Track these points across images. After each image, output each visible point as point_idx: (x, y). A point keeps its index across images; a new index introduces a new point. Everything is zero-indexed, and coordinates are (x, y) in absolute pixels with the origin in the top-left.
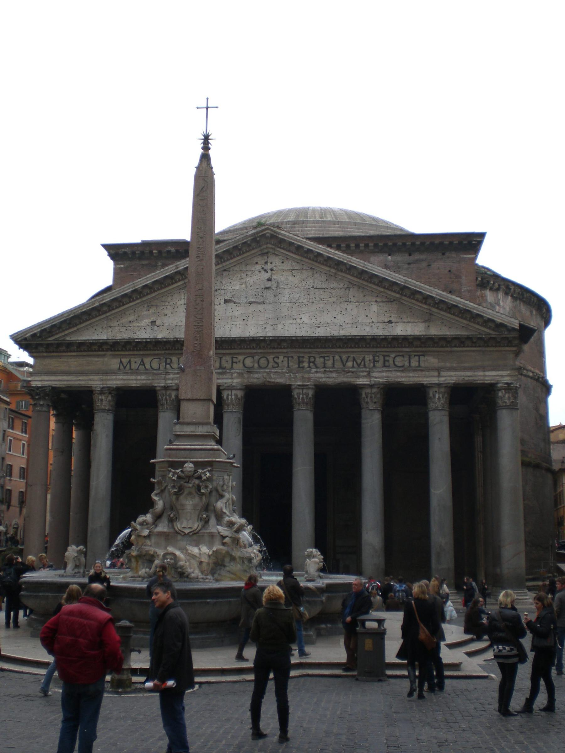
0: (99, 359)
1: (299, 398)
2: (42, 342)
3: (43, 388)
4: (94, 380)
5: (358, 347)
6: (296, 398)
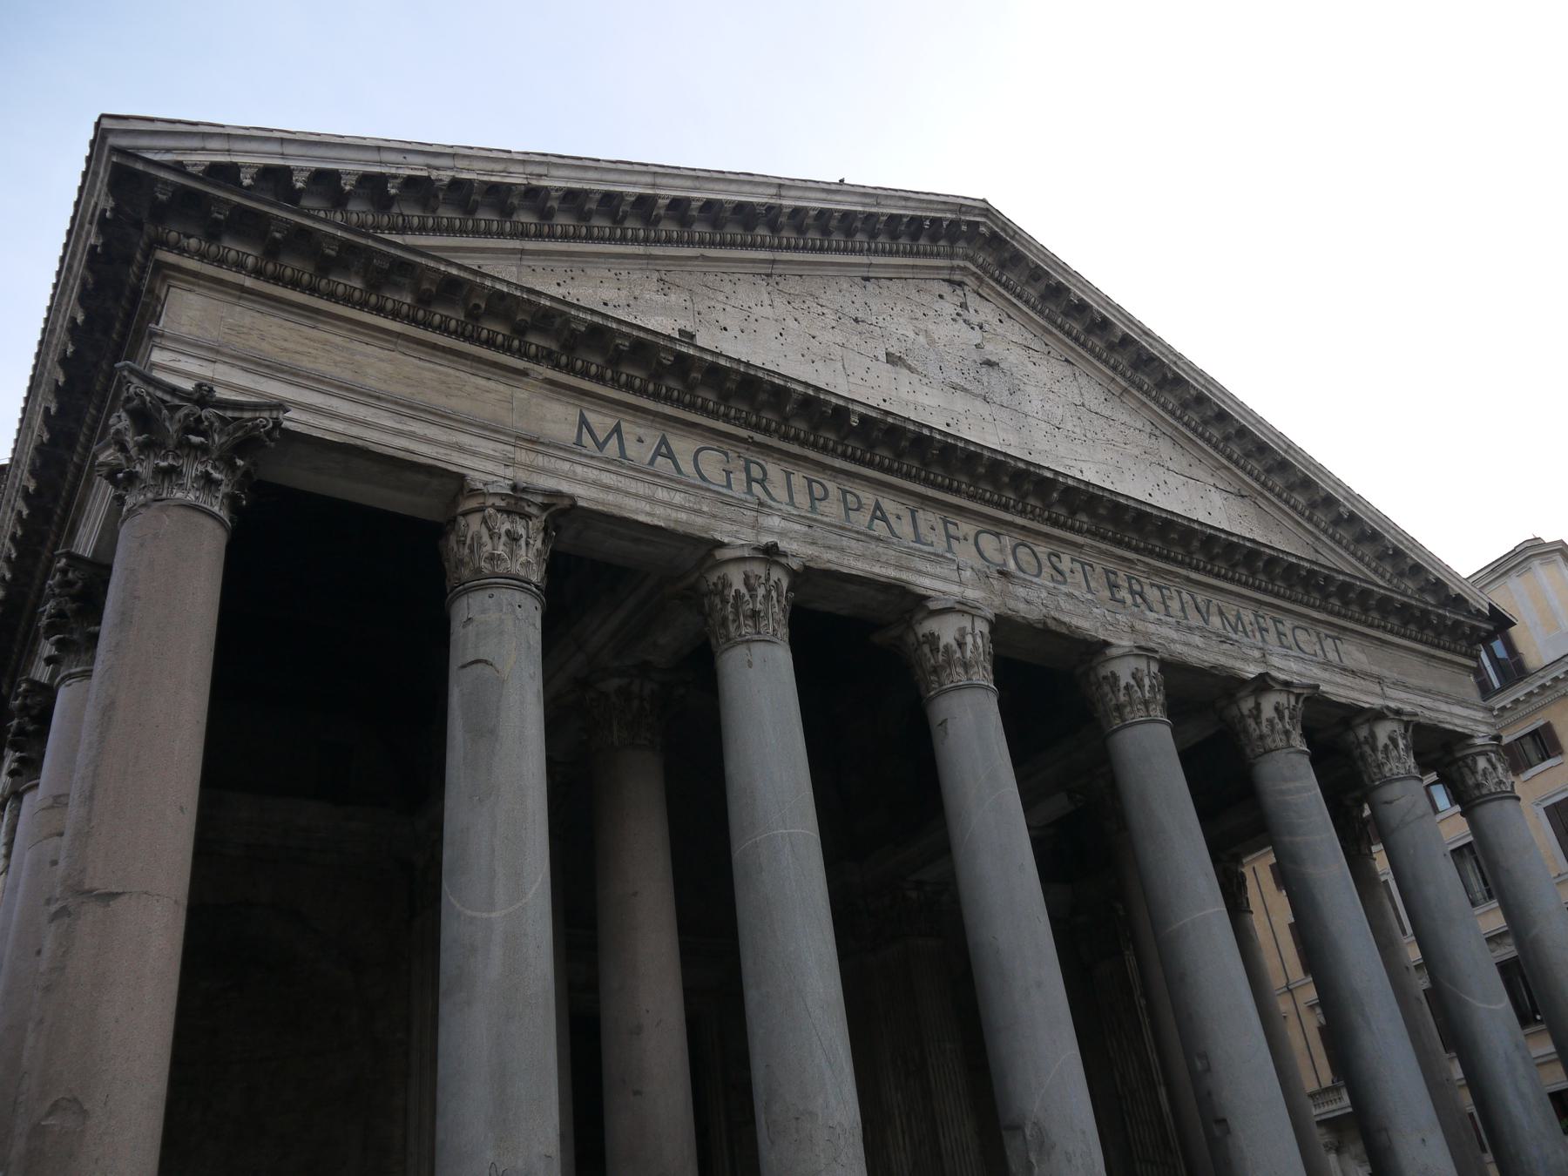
0: (491, 384)
1: (1141, 686)
2: (275, 212)
3: (229, 414)
4: (474, 454)
6: (1128, 687)
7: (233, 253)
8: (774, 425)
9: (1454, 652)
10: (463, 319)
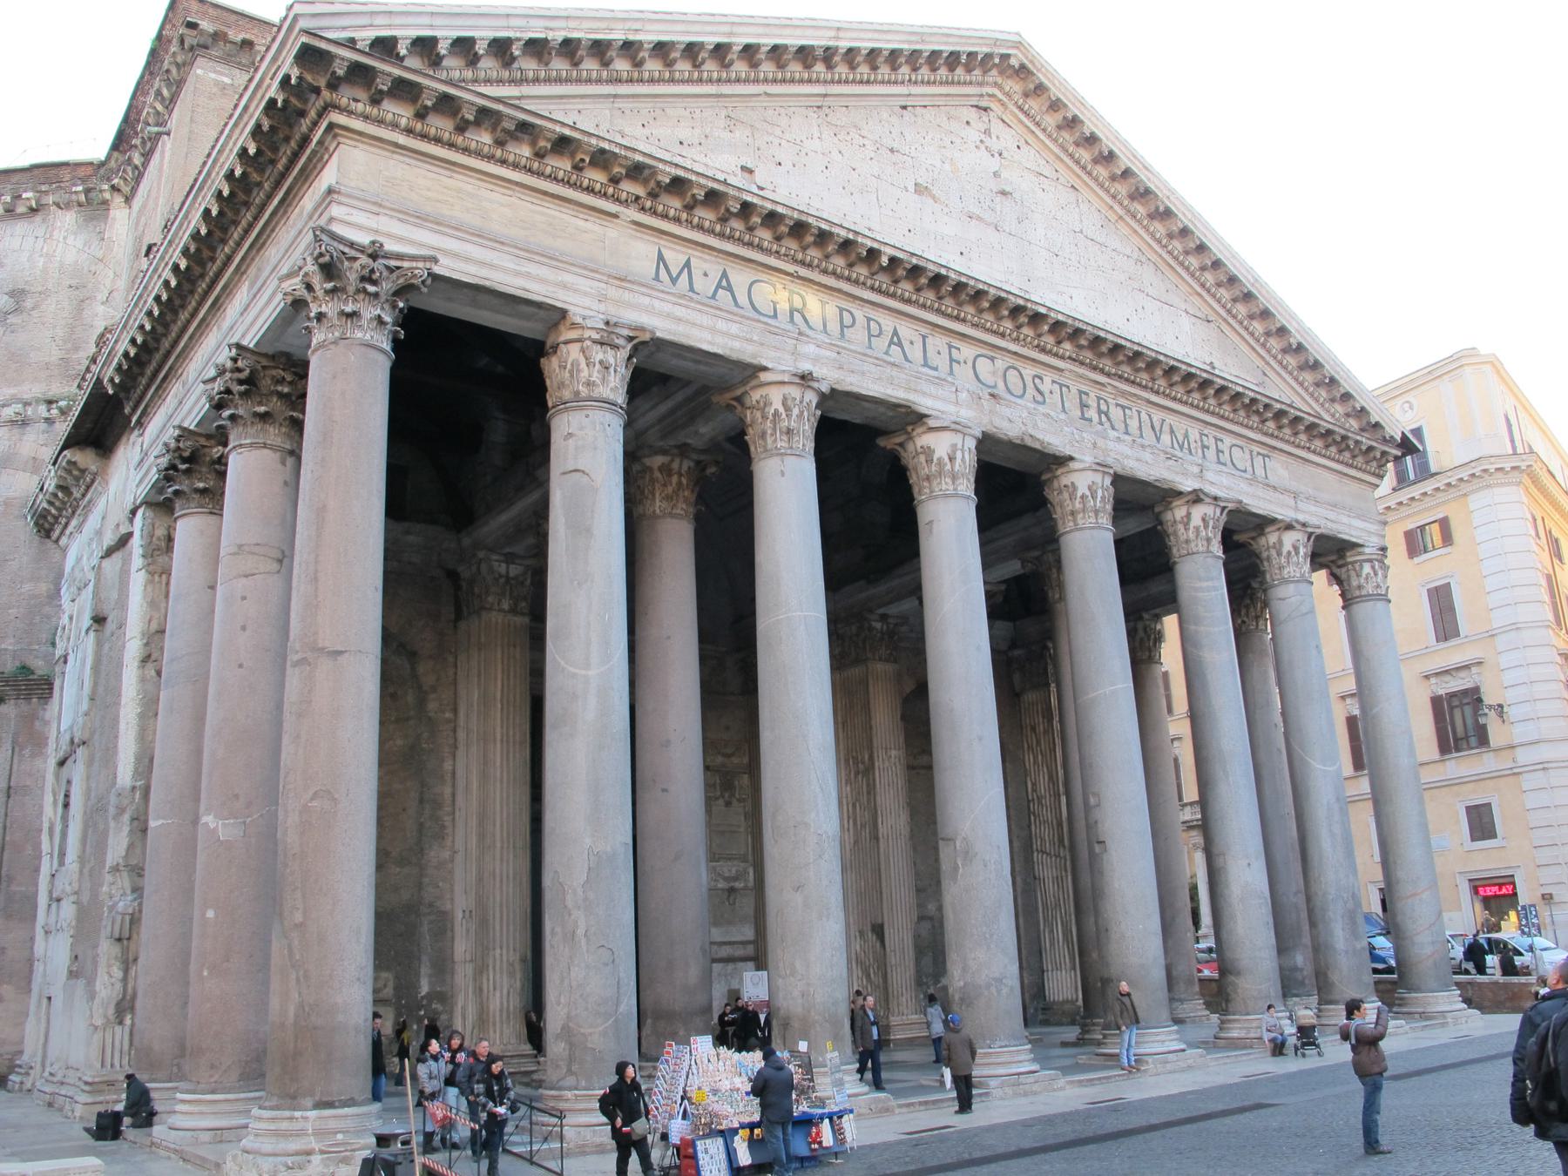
0: (589, 225)
4: (575, 291)
5: (1186, 403)
7: (390, 115)
8: (816, 261)
9: (1364, 471)
10: (569, 169)
